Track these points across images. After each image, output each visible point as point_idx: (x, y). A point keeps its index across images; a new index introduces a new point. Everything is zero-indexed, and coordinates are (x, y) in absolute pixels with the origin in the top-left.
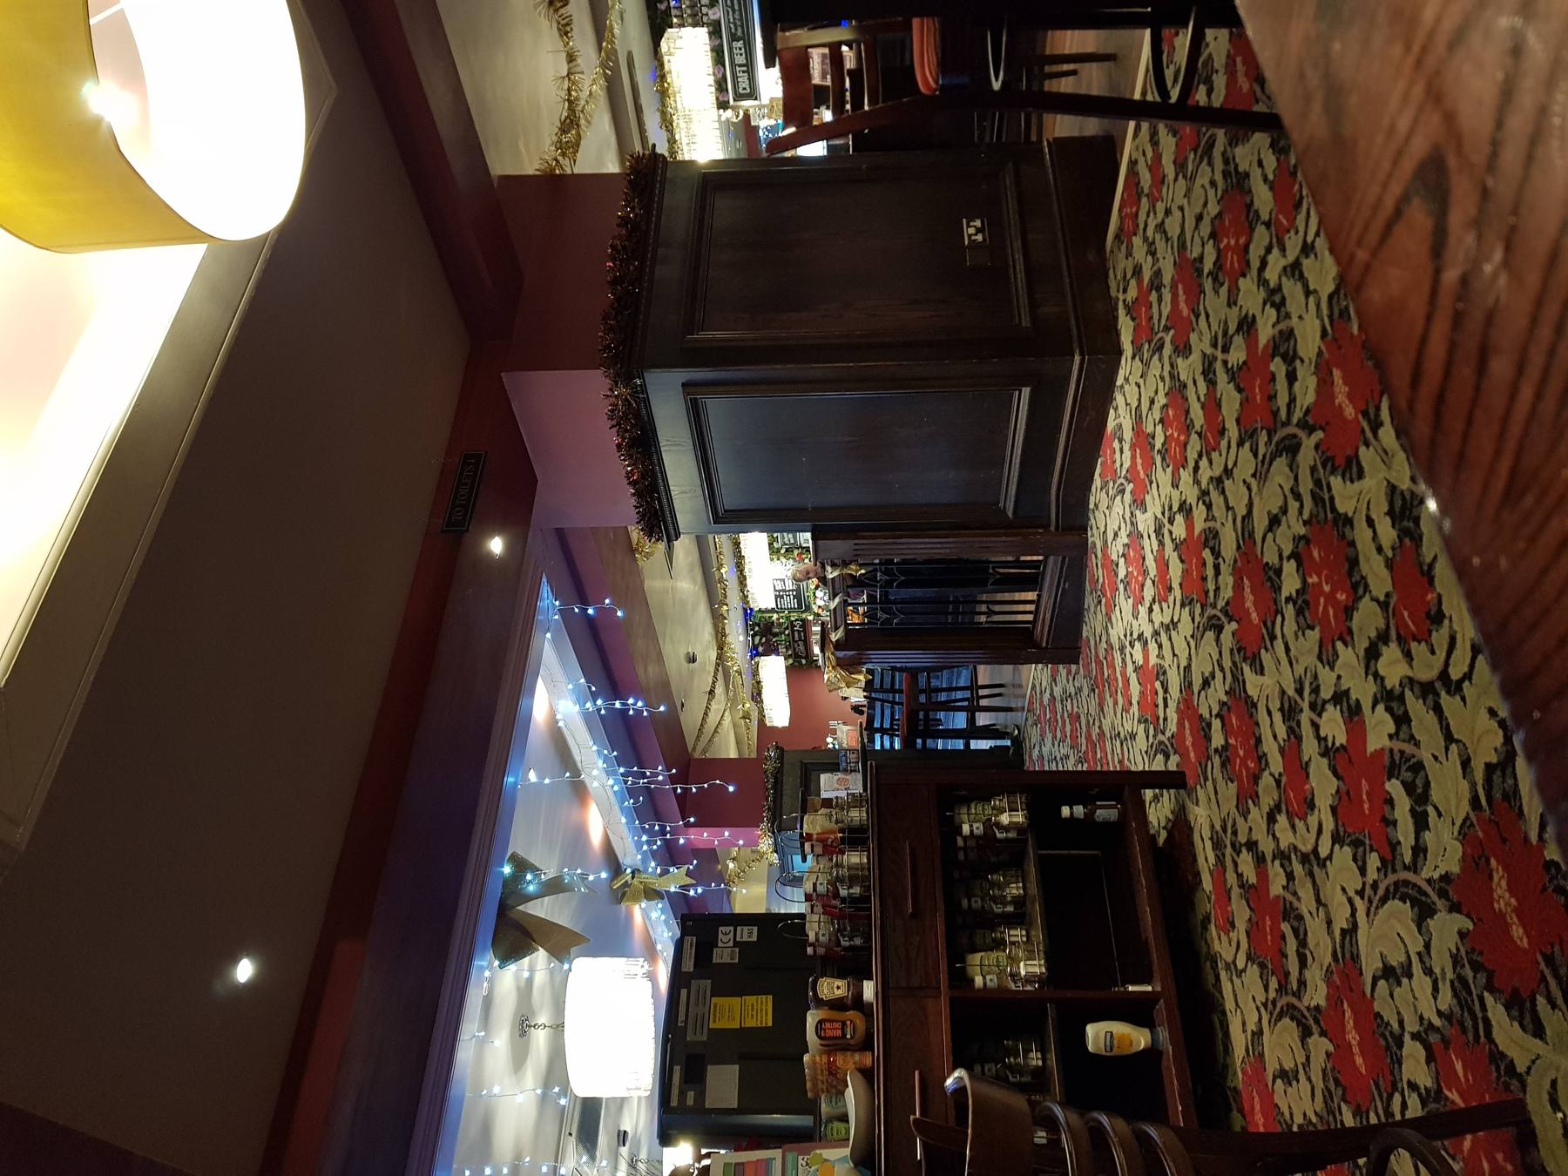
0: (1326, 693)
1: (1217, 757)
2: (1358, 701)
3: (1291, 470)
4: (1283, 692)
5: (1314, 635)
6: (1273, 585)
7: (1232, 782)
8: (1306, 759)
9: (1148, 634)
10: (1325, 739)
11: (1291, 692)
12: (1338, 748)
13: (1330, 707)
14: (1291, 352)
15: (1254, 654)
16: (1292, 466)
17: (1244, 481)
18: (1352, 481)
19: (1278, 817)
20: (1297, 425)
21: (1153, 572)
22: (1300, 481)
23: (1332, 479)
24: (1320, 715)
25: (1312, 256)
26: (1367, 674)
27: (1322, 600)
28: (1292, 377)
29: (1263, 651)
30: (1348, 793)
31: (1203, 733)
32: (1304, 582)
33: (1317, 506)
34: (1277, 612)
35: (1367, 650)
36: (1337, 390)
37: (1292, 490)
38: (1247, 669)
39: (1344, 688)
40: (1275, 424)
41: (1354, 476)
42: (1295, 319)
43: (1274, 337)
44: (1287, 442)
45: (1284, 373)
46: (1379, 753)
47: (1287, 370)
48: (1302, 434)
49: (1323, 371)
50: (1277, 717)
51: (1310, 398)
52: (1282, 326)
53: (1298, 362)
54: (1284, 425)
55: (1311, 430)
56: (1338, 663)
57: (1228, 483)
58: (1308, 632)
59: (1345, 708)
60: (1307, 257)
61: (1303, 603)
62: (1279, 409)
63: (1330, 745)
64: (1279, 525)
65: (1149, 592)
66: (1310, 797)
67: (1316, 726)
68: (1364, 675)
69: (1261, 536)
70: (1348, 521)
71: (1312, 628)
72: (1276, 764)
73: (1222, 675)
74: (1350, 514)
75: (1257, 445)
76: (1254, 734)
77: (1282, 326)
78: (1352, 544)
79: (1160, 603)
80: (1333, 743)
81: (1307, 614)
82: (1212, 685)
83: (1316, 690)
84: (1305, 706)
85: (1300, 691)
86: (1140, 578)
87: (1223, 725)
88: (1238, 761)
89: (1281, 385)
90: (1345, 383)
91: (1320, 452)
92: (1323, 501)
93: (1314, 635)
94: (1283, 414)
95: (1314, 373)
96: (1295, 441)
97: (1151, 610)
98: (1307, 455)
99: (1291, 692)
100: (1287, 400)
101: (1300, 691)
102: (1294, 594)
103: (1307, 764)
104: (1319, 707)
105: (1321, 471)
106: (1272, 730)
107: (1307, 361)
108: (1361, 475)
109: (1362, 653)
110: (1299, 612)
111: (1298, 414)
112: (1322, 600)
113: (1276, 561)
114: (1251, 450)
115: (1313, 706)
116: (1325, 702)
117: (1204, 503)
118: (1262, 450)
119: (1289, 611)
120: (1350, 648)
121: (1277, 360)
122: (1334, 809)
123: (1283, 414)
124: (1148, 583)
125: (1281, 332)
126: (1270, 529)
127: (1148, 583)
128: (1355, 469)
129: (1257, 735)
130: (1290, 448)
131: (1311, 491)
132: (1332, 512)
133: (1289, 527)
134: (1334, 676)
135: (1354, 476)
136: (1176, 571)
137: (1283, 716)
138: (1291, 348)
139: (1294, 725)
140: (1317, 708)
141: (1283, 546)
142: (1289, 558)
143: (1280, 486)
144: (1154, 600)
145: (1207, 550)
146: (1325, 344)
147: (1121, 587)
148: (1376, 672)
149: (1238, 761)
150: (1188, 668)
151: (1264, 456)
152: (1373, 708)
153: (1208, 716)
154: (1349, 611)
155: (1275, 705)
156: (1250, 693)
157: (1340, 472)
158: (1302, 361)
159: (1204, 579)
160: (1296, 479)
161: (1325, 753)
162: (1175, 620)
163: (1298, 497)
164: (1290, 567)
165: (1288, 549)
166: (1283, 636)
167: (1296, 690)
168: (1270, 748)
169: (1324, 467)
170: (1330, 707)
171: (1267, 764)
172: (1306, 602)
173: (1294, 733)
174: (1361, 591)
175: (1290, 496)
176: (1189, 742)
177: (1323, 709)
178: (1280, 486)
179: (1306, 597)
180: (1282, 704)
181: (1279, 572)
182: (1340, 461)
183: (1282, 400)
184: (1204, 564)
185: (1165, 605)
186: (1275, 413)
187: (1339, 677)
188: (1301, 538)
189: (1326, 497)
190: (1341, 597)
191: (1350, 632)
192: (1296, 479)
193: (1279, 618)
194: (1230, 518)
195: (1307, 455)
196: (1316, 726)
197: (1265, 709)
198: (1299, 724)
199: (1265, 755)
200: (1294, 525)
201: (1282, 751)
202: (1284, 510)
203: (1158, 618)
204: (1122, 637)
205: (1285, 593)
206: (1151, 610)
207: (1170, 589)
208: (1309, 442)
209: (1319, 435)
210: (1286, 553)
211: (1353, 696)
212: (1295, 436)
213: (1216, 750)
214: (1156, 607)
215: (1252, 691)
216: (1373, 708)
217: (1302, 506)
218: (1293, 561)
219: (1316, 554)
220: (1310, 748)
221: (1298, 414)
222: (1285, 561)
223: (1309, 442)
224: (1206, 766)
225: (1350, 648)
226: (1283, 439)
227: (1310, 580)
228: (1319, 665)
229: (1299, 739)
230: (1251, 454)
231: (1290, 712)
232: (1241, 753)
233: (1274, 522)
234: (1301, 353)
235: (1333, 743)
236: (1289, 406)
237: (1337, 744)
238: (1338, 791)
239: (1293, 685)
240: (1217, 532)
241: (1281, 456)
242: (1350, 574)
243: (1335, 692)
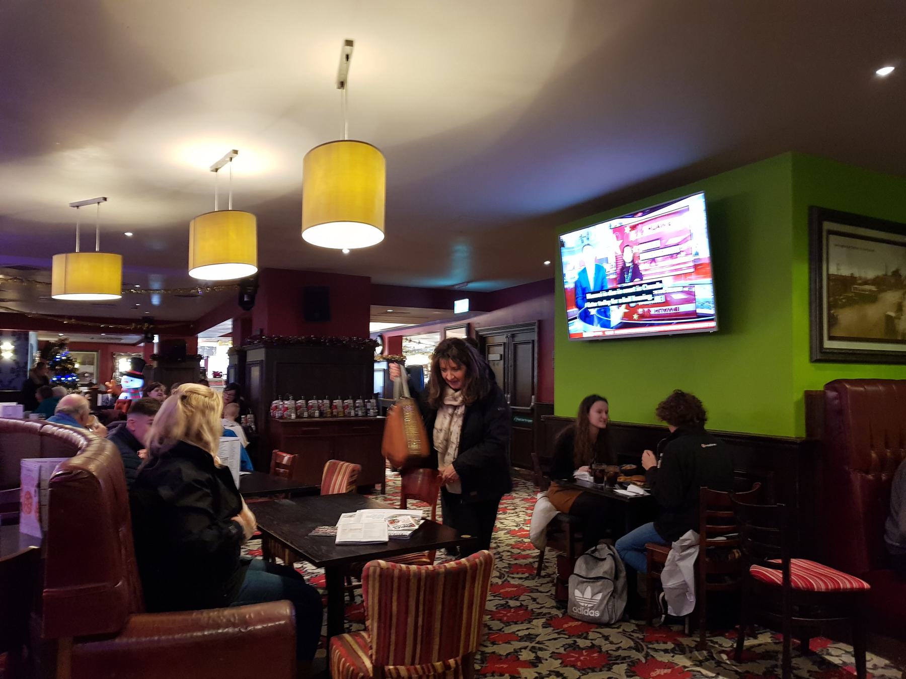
0: (540, 654)
1: (505, 603)
2: (538, 666)
3: (628, 648)
4: (537, 636)
5: (562, 650)
6: (580, 635)
7: (496, 609)
8: (512, 643)
9: (500, 550)
10: (521, 652)
11: (538, 639)
12: (517, 656)
13: (534, 655)
14: (676, 652)
15: (550, 624)
16: (630, 648)
17: (550, 590)
18: (626, 672)
19: (486, 629)
20: (647, 652)
21: (523, 553)
22: (624, 651)
23: (626, 665)
24: (530, 650)
25: (716, 665)
26: (550, 671)
27: (577, 656)
28: (666, 651)
29: (552, 629)
30: (501, 659)
31: (513, 596)
32: (583, 649)
33: (615, 657)
34: (569, 636)
35: (559, 672)
36: (662, 670)
37: (620, 647)
38: (544, 620)
39: (543, 661)
40: (646, 642)
41: (628, 674)
42: (690, 655)
43: (683, 645)
44: (640, 647)
45: (668, 648)
46: (519, 673)
47: (668, 649)
48: (644, 653)
49: (670, 665)
50: (526, 632)
51: (659, 659)
52: (687, 649)
53: (672, 655)
54: (646, 646)
55: (646, 658)
56: (553, 660)
57: (550, 585)
58: (563, 648)
59: (536, 661)
60: (715, 663)
61: (574, 647)
62: (653, 644)
63: (519, 653)
64: (605, 640)
65: (516, 551)
66: (497, 643)
67: (525, 648)
68: (549, 670)
69: (601, 632)
70: (610, 669)
71: (565, 650)
72: (508, 630)
73: (539, 607)
74: (612, 670)
75: (636, 633)
76: (518, 621)
77: (687, 649)
78: (601, 671)
79: (511, 555)
80: (520, 655)
81: (570, 649)
82: (534, 602)
83: (541, 649)
84: (533, 644)
85: (538, 643)
86: (522, 548)
87: (518, 606)
88: (505, 612)
89: (662, 646)
90: (665, 674)
91: (637, 661)
92: (617, 660)
93: (562, 650)
94: (650, 646)
95: (669, 661)
96: (641, 650)
97: (509, 551)
98: (635, 655)
99: (538, 639)
100: (657, 648)
101: (538, 643)
102: (577, 644)
103: (509, 643)
104: (534, 651)
105: (629, 660)
106: (521, 629)
107: (673, 659)
108: (628, 676)
109: (556, 670)
110: (570, 646)
111: (652, 653)
112: (577, 656)
113: (590, 638)
114: (634, 630)
115: (533, 647)
116: (536, 653)
117: (545, 575)
118: (635, 635)
119: (570, 641)
120: (560, 665)
121: (673, 646)
122: (494, 653)
123: (650, 646)
124: (519, 551)
125: (685, 648)
126: (604, 636)
127: (519, 551)
128: (631, 674)
129: (518, 623)
130: (638, 649)
131: (620, 655)
132: (612, 663)
133: (605, 644)
134: (547, 657)
135: (628, 674)
136: (522, 562)
137: (527, 635)
138: (676, 652)
139: (525, 639)
140: (533, 649)
141: (596, 641)
142: (592, 643)
143: (621, 642)
144: (512, 553)
145: (528, 575)
146: (681, 667)
147: (520, 540)
148: (551, 675)
149: (505, 612)
150: (538, 591)
151: (632, 636)
152: (536, 672)
153: (520, 599)
154: (574, 666)
155: (530, 631)
156: (534, 621)
157: (629, 668)
158: (673, 656)
159: (518, 574)
160: (625, 649)
161: (516, 651)
162: (503, 561)
163: (618, 649)
164: (588, 643)
165: (596, 642)
166: (560, 638)
167: (539, 641)
168: (514, 628)
169: (631, 661)
170: (534, 655)
171: (507, 626)
172: (574, 649)
173: (521, 639)
174: (583, 672)
175: (618, 646)
176: (507, 589)
177: (533, 652)
178: (621, 642)
179: (577, 649)
180: (532, 635)
181: (586, 638)
182: (633, 669)
183: (656, 646)
184: (523, 574)
185: (509, 557)
186: (651, 643)
187: (547, 660)
188: (601, 649)
189: (618, 662)
190: (579, 664)
191: (566, 666)
192: (625, 649)
193: (567, 637)
194: (538, 585)
195: (635, 655)
196: (525, 648)
197: (529, 627)
198: (526, 641)
199: (510, 625)
200: (606, 647)
201: (514, 633)
202: (611, 643)
203: (505, 554)
204: (499, 539)
205: (578, 640)
206: (509, 551)
207: (516, 559)
208: (641, 656)
209: (644, 661)
210: (593, 642)
211: (540, 665)
212: (643, 650)
213: (507, 602)
214: (509, 554)
215: (535, 622)
216: (536, 672)
217: (614, 651)
218: (591, 644)
219: (595, 655)
220: (517, 645)
221: (652, 653)
222: (590, 641)
223: (641, 656)
224: (500, 597)
225: (560, 665)
226: (641, 645)
227: (584, 651)
228: (551, 652)
229: (520, 641)
230: (632, 630)
231: (529, 637)
232: (509, 614)
233: (606, 638)
234: (677, 656)
235: (520, 655)
236: (654, 649)
237: (520, 657)
238: (500, 655)
239: (541, 640)
240: (533, 579)
241: (635, 644)
242: (589, 668)
243: (541, 658)
